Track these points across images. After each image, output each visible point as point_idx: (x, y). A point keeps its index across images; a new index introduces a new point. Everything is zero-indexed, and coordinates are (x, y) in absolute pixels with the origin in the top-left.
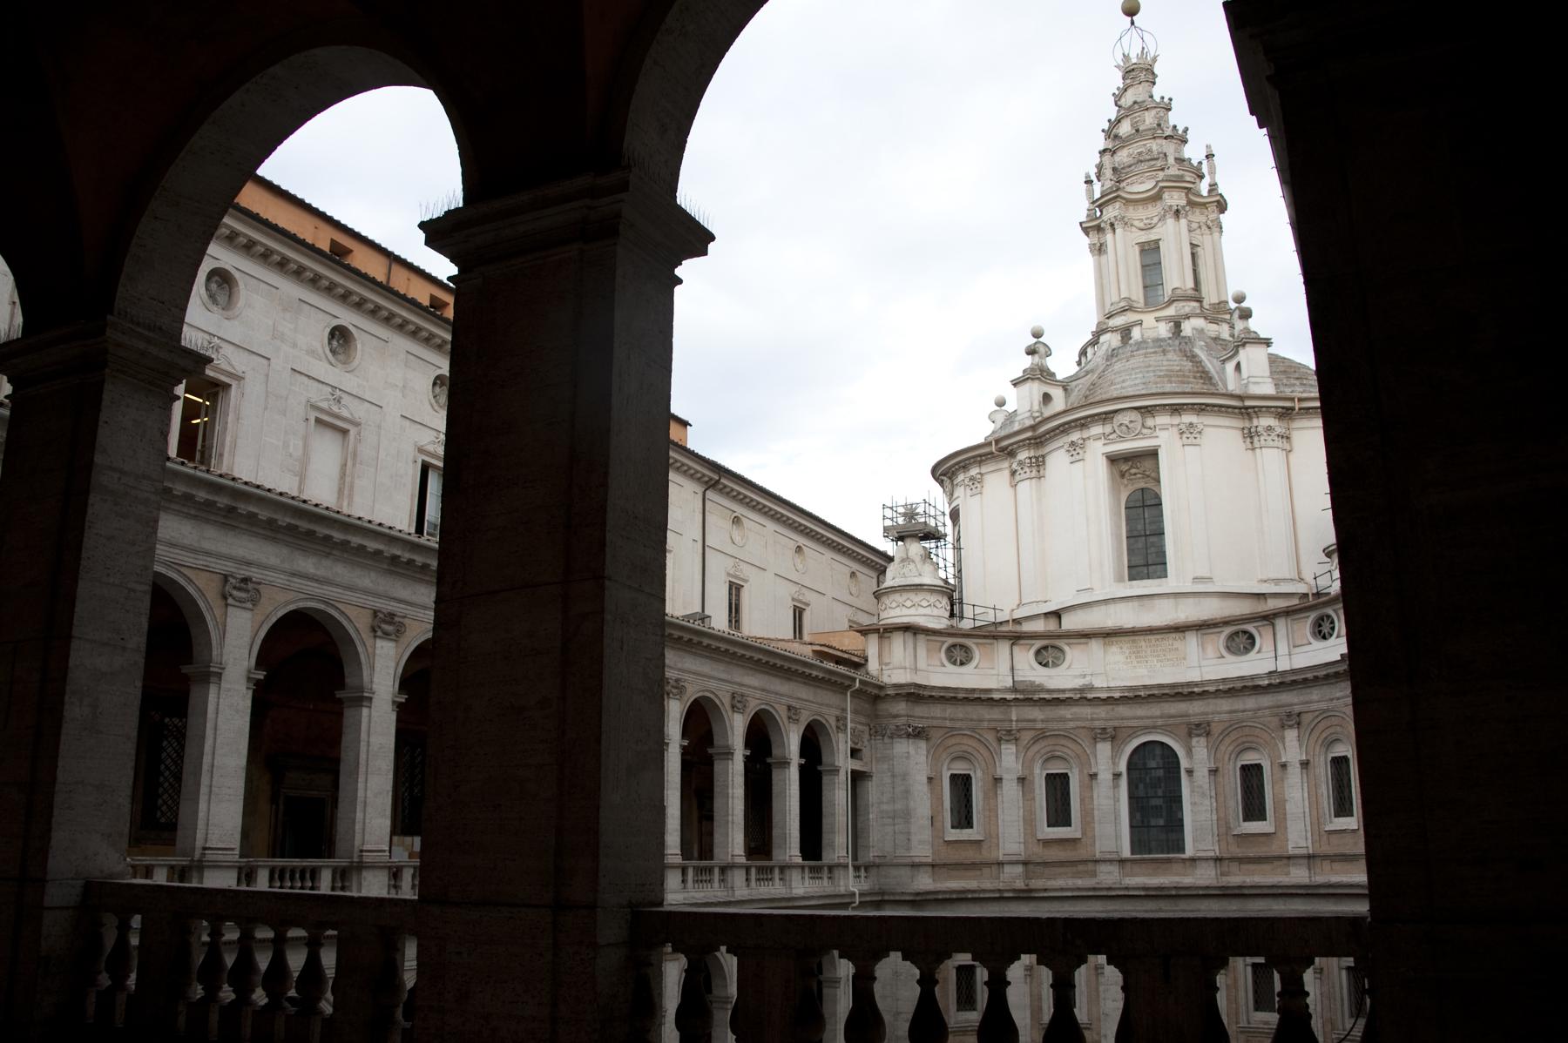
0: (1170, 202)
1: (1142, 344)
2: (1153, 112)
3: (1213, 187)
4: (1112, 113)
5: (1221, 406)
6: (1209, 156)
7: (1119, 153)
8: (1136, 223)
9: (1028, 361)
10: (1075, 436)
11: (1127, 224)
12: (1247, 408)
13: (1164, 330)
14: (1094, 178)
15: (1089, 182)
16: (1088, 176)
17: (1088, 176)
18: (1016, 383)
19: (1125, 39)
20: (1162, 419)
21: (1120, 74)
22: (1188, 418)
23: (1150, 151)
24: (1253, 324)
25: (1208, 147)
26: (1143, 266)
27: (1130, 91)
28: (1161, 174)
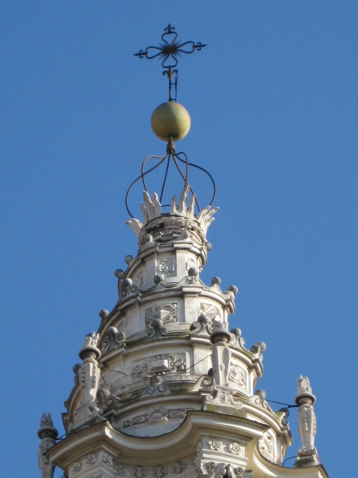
17: (47, 420)
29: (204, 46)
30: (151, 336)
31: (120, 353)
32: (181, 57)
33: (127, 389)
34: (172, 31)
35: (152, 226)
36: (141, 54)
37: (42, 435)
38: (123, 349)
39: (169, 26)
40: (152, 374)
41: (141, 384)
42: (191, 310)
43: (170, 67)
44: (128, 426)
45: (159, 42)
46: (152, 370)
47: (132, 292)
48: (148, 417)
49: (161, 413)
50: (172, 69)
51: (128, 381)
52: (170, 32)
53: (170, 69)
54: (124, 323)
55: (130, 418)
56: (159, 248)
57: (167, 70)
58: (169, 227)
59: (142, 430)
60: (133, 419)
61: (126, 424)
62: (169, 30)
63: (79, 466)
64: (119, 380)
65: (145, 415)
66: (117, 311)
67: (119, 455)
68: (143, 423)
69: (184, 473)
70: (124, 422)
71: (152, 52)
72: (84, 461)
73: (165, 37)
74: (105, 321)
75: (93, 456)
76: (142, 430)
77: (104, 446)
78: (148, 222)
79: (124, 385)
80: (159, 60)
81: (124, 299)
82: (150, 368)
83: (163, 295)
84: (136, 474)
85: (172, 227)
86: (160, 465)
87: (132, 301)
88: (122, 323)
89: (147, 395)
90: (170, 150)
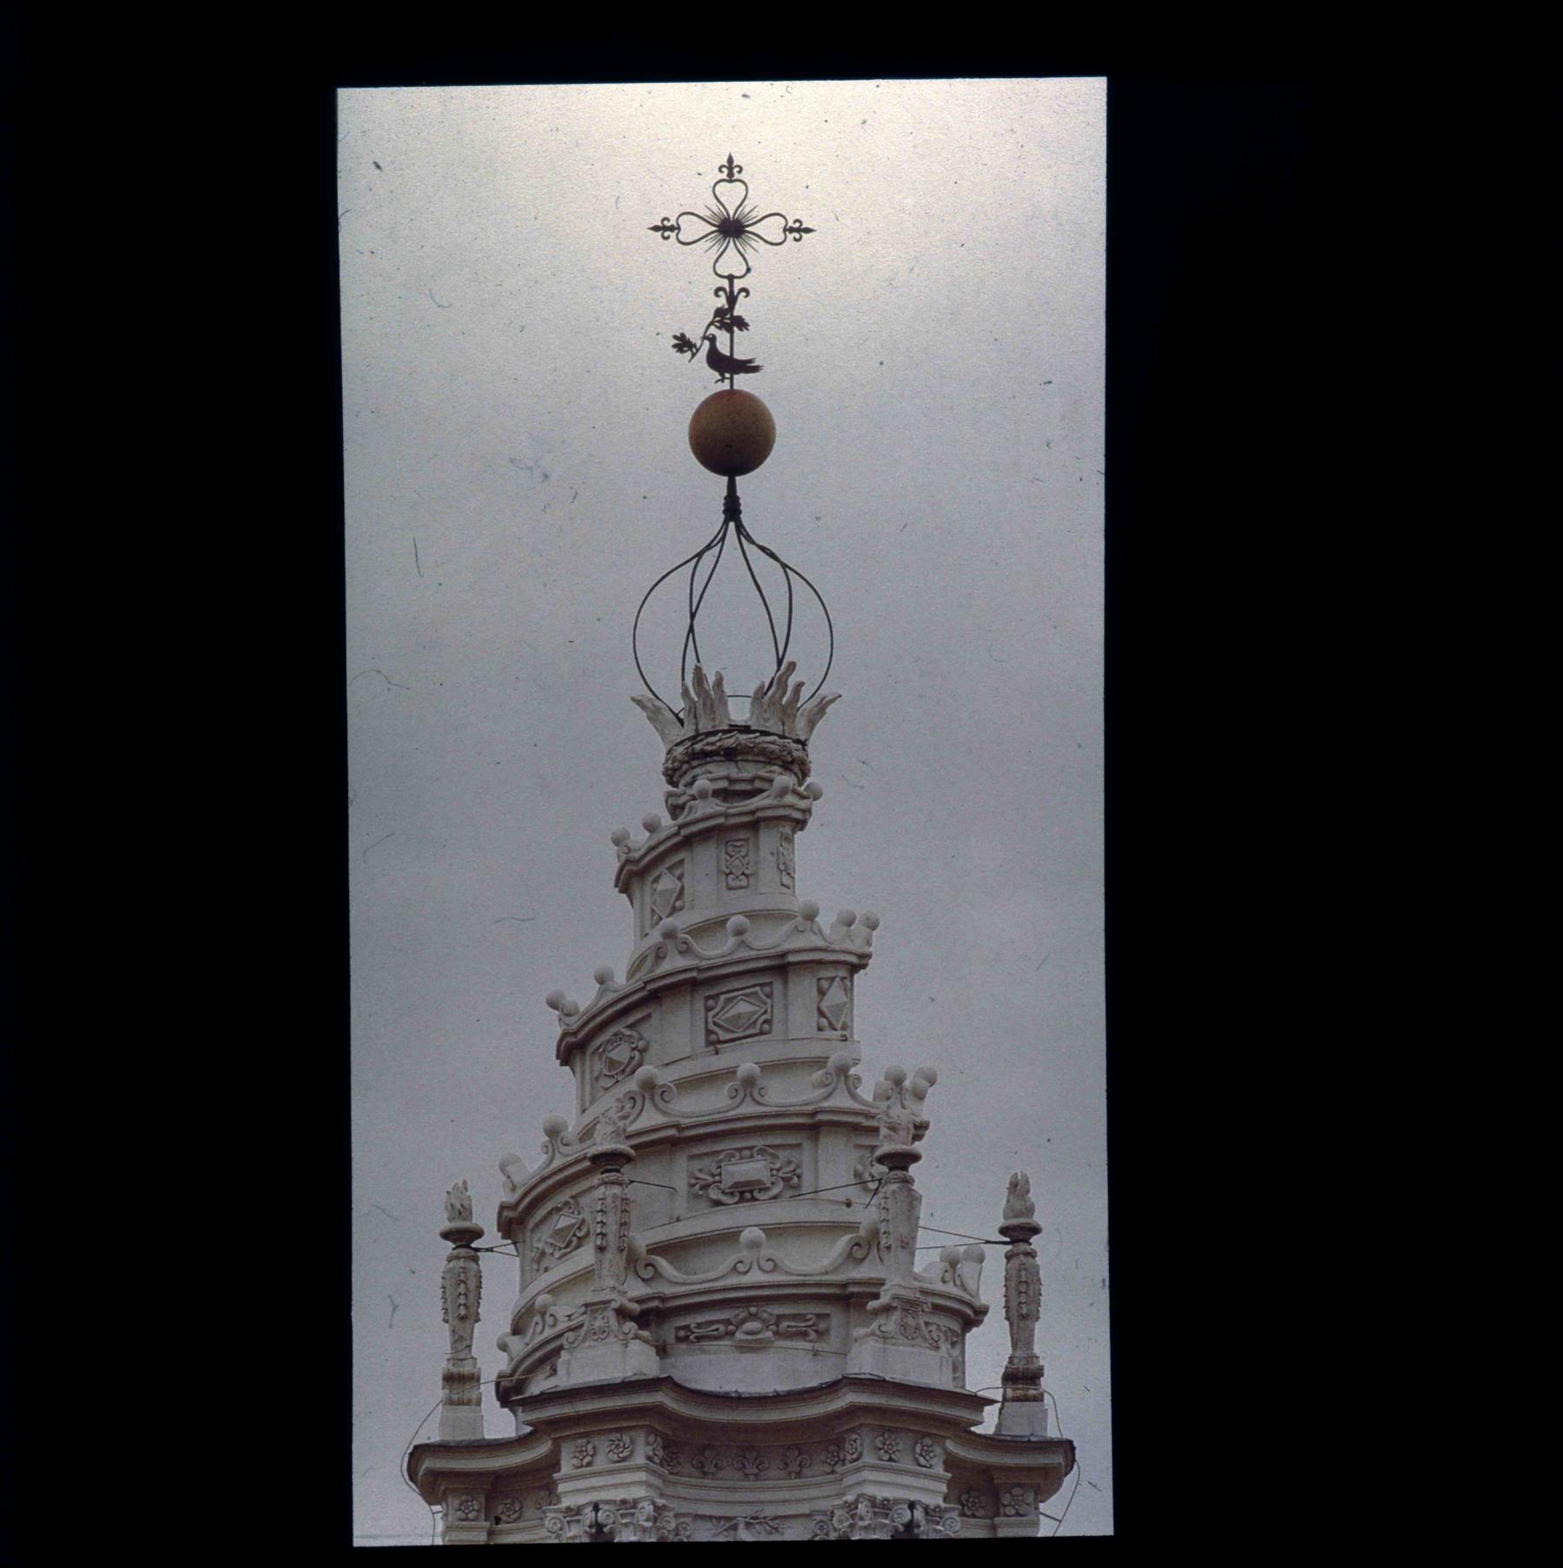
14: (486, 1218)
15: (463, 1237)
16: (462, 1211)
21: (654, 751)
32: (758, 254)
34: (737, 176)
36: (664, 228)
39: (730, 160)
40: (732, 1194)
43: (731, 278)
45: (704, 204)
48: (731, 1328)
49: (764, 1321)
50: (738, 284)
52: (731, 179)
53: (731, 285)
61: (682, 1333)
62: (731, 170)
65: (727, 1322)
70: (678, 1329)
71: (692, 228)
73: (723, 189)
80: (705, 252)
88: (649, 1016)
90: (732, 509)
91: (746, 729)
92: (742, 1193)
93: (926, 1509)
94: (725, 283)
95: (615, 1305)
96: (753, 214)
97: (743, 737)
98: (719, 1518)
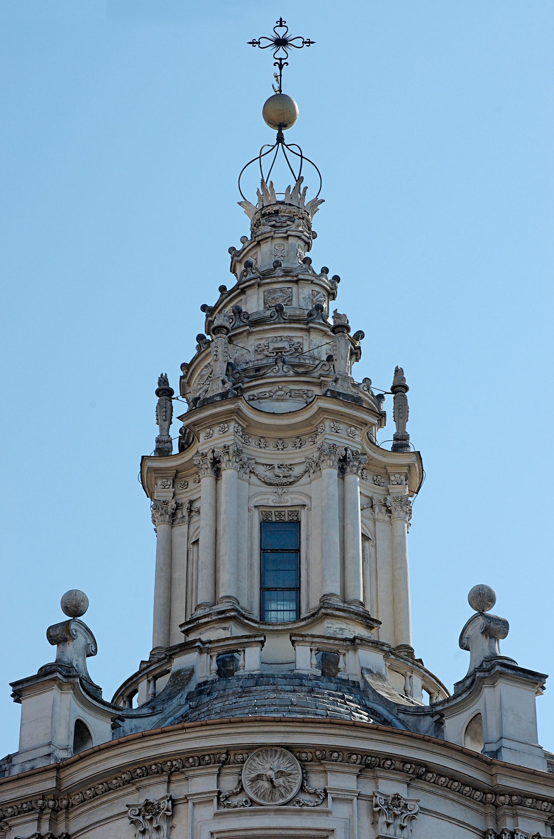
0: (333, 439)
1: (258, 679)
2: (306, 291)
3: (401, 443)
4: (231, 282)
5: (453, 777)
6: (399, 388)
7: (240, 342)
8: (260, 470)
9: (49, 654)
10: (156, 792)
11: (246, 467)
12: (496, 794)
13: (305, 660)
15: (164, 392)
16: (163, 380)
17: (163, 380)
18: (20, 691)
19: (267, 161)
20: (342, 780)
22: (390, 787)
23: (298, 350)
24: (505, 648)
25: (398, 372)
26: (263, 550)
27: (266, 247)
28: (317, 391)
29: (313, 43)
30: (274, 318)
31: (245, 331)
33: (251, 365)
34: (283, 24)
35: (267, 212)
37: (160, 393)
38: (248, 327)
39: (281, 19)
40: (273, 353)
41: (264, 362)
42: (304, 296)
43: (281, 59)
44: (253, 399)
45: (271, 34)
46: (273, 350)
47: (253, 273)
48: (272, 394)
50: (283, 61)
51: (252, 357)
52: (281, 25)
53: (281, 62)
54: (244, 301)
55: (255, 392)
56: (275, 233)
57: (278, 61)
58: (282, 214)
59: (266, 405)
60: (258, 394)
61: (251, 397)
62: (281, 23)
63: (211, 432)
64: (243, 355)
65: (271, 392)
66: (238, 289)
67: (247, 426)
68: (266, 398)
69: (303, 449)
71: (264, 43)
72: (216, 429)
74: (224, 296)
75: (226, 425)
76: (266, 405)
77: (235, 417)
78: (263, 207)
79: (248, 361)
80: (271, 50)
81: (244, 279)
82: (271, 348)
83: (281, 279)
84: (260, 444)
85: (286, 214)
86: (281, 439)
87: (253, 282)
89: (272, 374)
90: (280, 139)
91: (282, 203)
92: (277, 353)
93: (352, 451)
94: (278, 61)
95: (221, 378)
96: (290, 37)
97: (283, 207)
98: (267, 465)
